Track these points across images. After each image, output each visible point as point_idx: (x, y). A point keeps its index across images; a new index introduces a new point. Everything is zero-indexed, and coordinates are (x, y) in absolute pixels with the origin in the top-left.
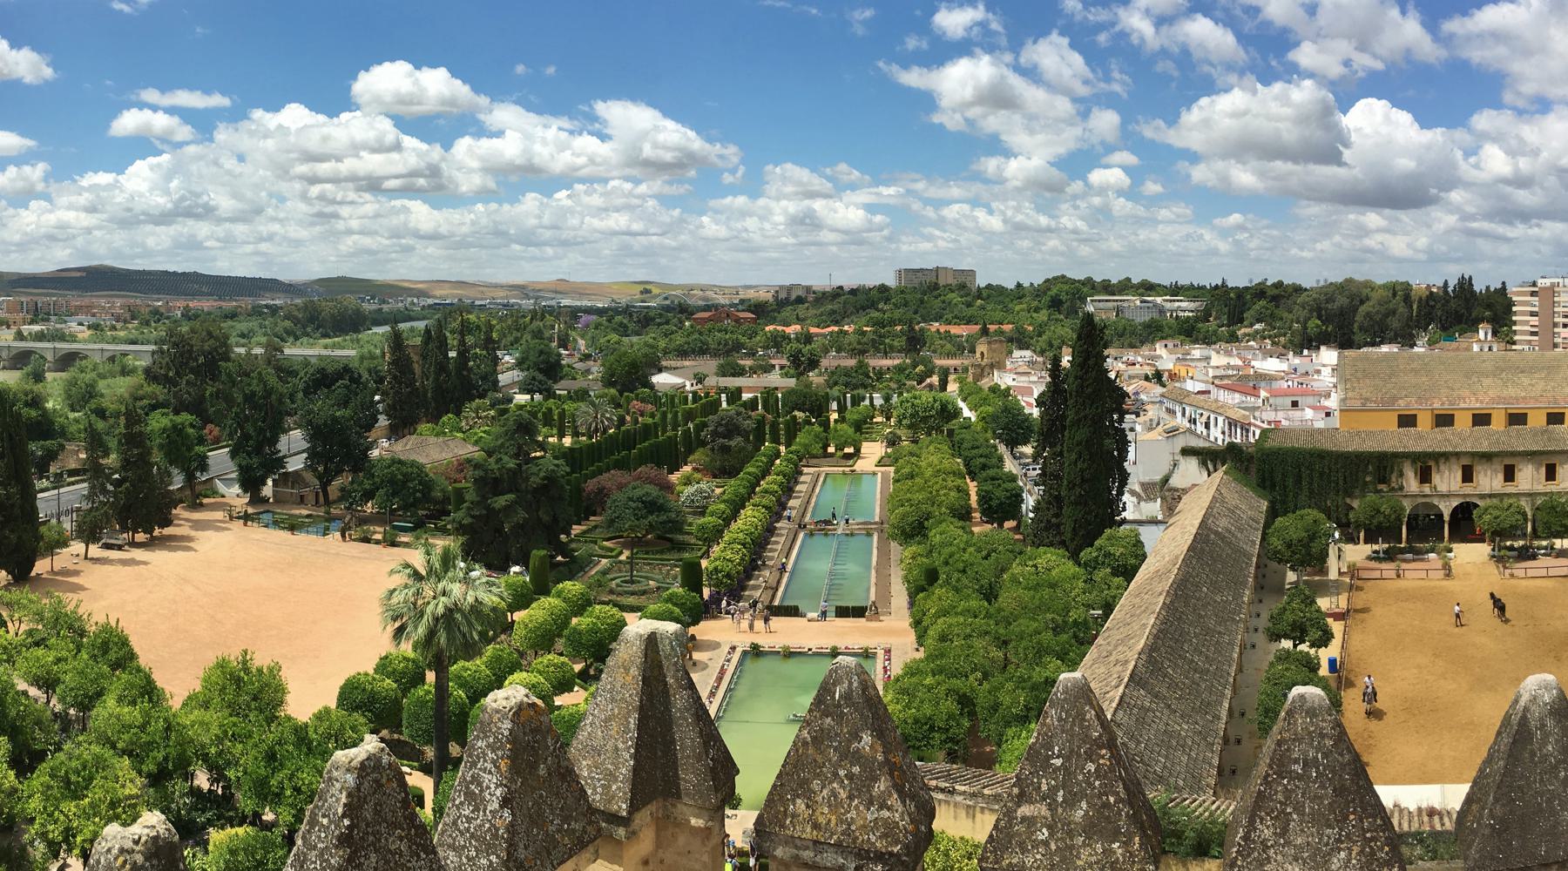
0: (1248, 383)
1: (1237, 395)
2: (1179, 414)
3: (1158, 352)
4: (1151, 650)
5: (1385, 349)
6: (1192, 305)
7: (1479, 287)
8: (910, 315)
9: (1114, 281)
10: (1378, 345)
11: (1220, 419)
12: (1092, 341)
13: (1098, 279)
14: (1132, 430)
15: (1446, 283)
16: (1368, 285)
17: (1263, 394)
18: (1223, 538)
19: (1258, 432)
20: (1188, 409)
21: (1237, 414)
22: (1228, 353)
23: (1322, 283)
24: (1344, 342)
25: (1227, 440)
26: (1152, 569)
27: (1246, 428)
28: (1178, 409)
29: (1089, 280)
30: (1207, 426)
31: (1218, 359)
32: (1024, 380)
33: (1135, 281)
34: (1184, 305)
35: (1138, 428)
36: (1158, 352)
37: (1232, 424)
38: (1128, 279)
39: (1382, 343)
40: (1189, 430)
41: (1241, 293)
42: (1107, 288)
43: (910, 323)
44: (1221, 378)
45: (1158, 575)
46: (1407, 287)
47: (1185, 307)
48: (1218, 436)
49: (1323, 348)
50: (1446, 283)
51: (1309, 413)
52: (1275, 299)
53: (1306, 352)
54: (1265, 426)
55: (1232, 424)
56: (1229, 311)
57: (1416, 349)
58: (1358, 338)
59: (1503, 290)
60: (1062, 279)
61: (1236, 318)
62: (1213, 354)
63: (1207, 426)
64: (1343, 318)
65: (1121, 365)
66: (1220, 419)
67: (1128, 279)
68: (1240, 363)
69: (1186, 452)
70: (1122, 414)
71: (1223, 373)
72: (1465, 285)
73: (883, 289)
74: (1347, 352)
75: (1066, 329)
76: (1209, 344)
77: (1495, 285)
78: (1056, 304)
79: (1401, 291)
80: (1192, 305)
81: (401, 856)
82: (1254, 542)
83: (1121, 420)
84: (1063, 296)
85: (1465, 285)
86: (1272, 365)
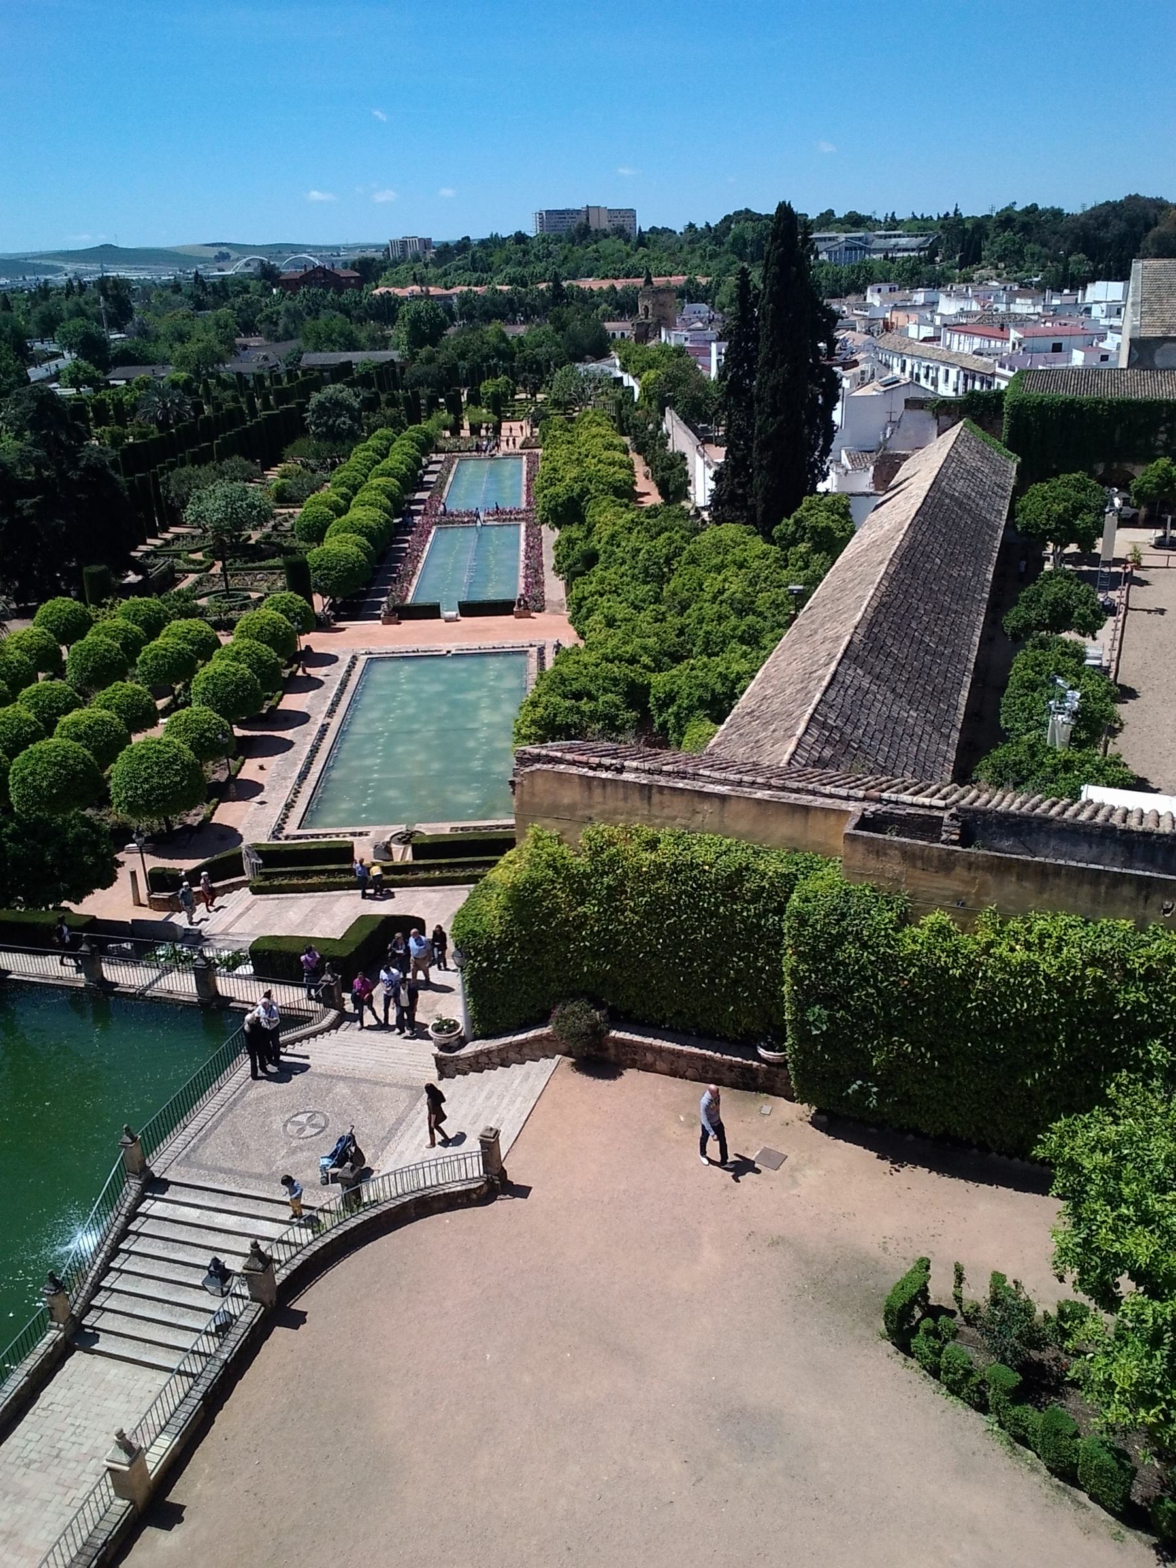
11: (953, 373)
20: (909, 362)
63: (935, 383)
66: (953, 373)
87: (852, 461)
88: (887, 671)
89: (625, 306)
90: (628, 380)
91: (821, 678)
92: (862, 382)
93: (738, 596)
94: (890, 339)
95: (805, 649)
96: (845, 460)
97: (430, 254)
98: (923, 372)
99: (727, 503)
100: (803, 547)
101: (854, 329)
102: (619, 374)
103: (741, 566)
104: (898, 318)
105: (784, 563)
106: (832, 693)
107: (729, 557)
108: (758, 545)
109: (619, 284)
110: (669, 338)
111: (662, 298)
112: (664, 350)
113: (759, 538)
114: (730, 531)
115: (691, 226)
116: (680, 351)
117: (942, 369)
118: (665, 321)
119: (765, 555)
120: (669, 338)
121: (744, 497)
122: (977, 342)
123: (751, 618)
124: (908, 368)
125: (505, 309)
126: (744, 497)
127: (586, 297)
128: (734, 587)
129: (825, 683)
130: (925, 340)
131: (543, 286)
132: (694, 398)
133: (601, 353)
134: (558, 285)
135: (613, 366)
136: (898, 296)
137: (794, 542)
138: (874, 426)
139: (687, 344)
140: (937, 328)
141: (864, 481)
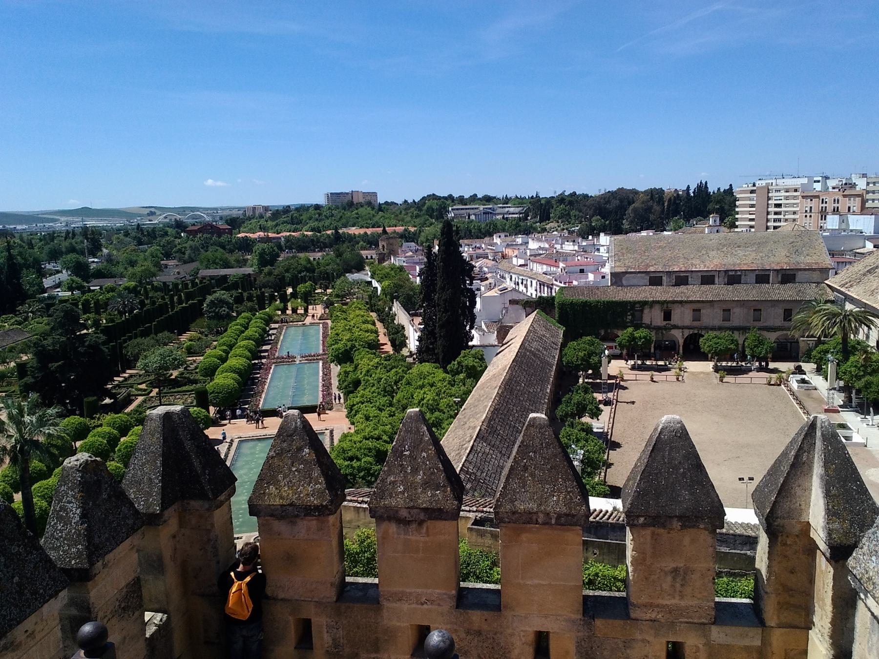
0: (553, 258)
1: (545, 267)
2: (508, 280)
3: (495, 241)
4: (490, 421)
5: (644, 233)
6: (517, 210)
7: (712, 189)
8: (335, 224)
9: (467, 196)
10: (639, 231)
11: (534, 282)
12: (451, 237)
13: (456, 195)
14: (478, 289)
15: (688, 187)
16: (635, 192)
17: (561, 265)
18: (535, 355)
19: (558, 288)
20: (514, 277)
21: (545, 279)
22: (540, 240)
23: (603, 192)
24: (615, 230)
25: (539, 294)
26: (491, 374)
27: (550, 287)
28: (507, 276)
29: (450, 196)
30: (526, 286)
31: (533, 245)
32: (409, 262)
33: (480, 196)
34: (512, 210)
35: (483, 289)
36: (495, 241)
37: (542, 284)
38: (476, 195)
39: (642, 229)
40: (514, 289)
41: (549, 201)
42: (462, 200)
43: (336, 229)
44: (535, 256)
45: (494, 376)
46: (661, 191)
47: (514, 212)
48: (532, 292)
49: (602, 235)
50: (688, 187)
51: (591, 277)
52: (571, 203)
53: (590, 237)
54: (562, 285)
55: (542, 284)
56: (539, 213)
57: (665, 233)
58: (626, 225)
59: (730, 191)
60: (433, 197)
61: (545, 217)
62: (530, 240)
63: (526, 286)
64: (616, 213)
65: (466, 251)
66: (534, 282)
67: (476, 195)
68: (547, 246)
69: (512, 302)
70: (472, 279)
71: (537, 252)
72: (702, 189)
73: (317, 207)
74: (616, 237)
75: (435, 228)
76: (528, 234)
77: (724, 187)
78: (430, 212)
79: (656, 195)
80: (517, 210)
81: (20, 555)
82: (554, 357)
83: (471, 284)
84: (434, 208)
85: (702, 189)
86: (569, 247)
87: (487, 327)
88: (498, 443)
89: (372, 242)
90: (375, 284)
91: (466, 449)
92: (490, 288)
93: (431, 402)
94: (504, 264)
95: (461, 432)
96: (484, 327)
97: (269, 214)
98: (520, 281)
99: (425, 353)
100: (462, 376)
101: (487, 258)
102: (370, 280)
103: (432, 385)
104: (509, 252)
105: (452, 384)
106: (471, 456)
107: (426, 381)
108: (440, 374)
109: (369, 231)
110: (396, 261)
111: (391, 241)
112: (393, 268)
113: (441, 370)
114: (427, 367)
115: (406, 201)
116: (401, 269)
117: (529, 280)
118: (393, 252)
119: (444, 379)
120: (396, 261)
121: (433, 349)
122: (545, 268)
123: (437, 414)
124: (513, 279)
125: (305, 245)
126: (433, 349)
127: (352, 239)
128: (428, 397)
129: (468, 451)
130: (520, 266)
131: (329, 232)
132: (408, 295)
133: (360, 268)
134: (337, 232)
135: (366, 275)
136: (509, 239)
137: (458, 373)
138: (497, 309)
139: (405, 264)
140: (526, 260)
141: (493, 339)
